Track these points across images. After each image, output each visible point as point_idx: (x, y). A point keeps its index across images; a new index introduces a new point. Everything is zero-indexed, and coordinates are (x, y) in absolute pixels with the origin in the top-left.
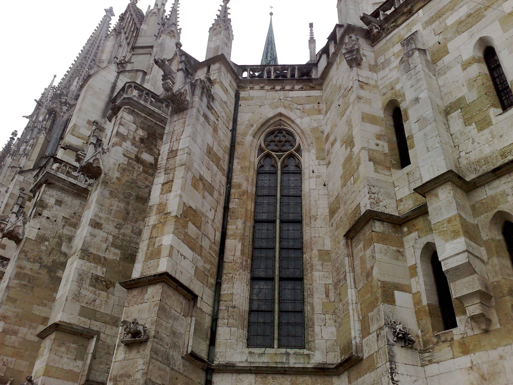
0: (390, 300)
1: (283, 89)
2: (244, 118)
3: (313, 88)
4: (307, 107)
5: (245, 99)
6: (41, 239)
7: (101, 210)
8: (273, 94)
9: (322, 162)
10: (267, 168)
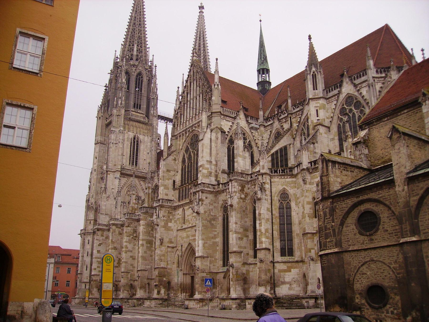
0: (310, 252)
1: (284, 178)
2: (274, 190)
3: (293, 178)
4: (292, 185)
5: (273, 182)
6: (205, 212)
7: (236, 219)
8: (281, 180)
9: (297, 206)
10: (281, 207)
